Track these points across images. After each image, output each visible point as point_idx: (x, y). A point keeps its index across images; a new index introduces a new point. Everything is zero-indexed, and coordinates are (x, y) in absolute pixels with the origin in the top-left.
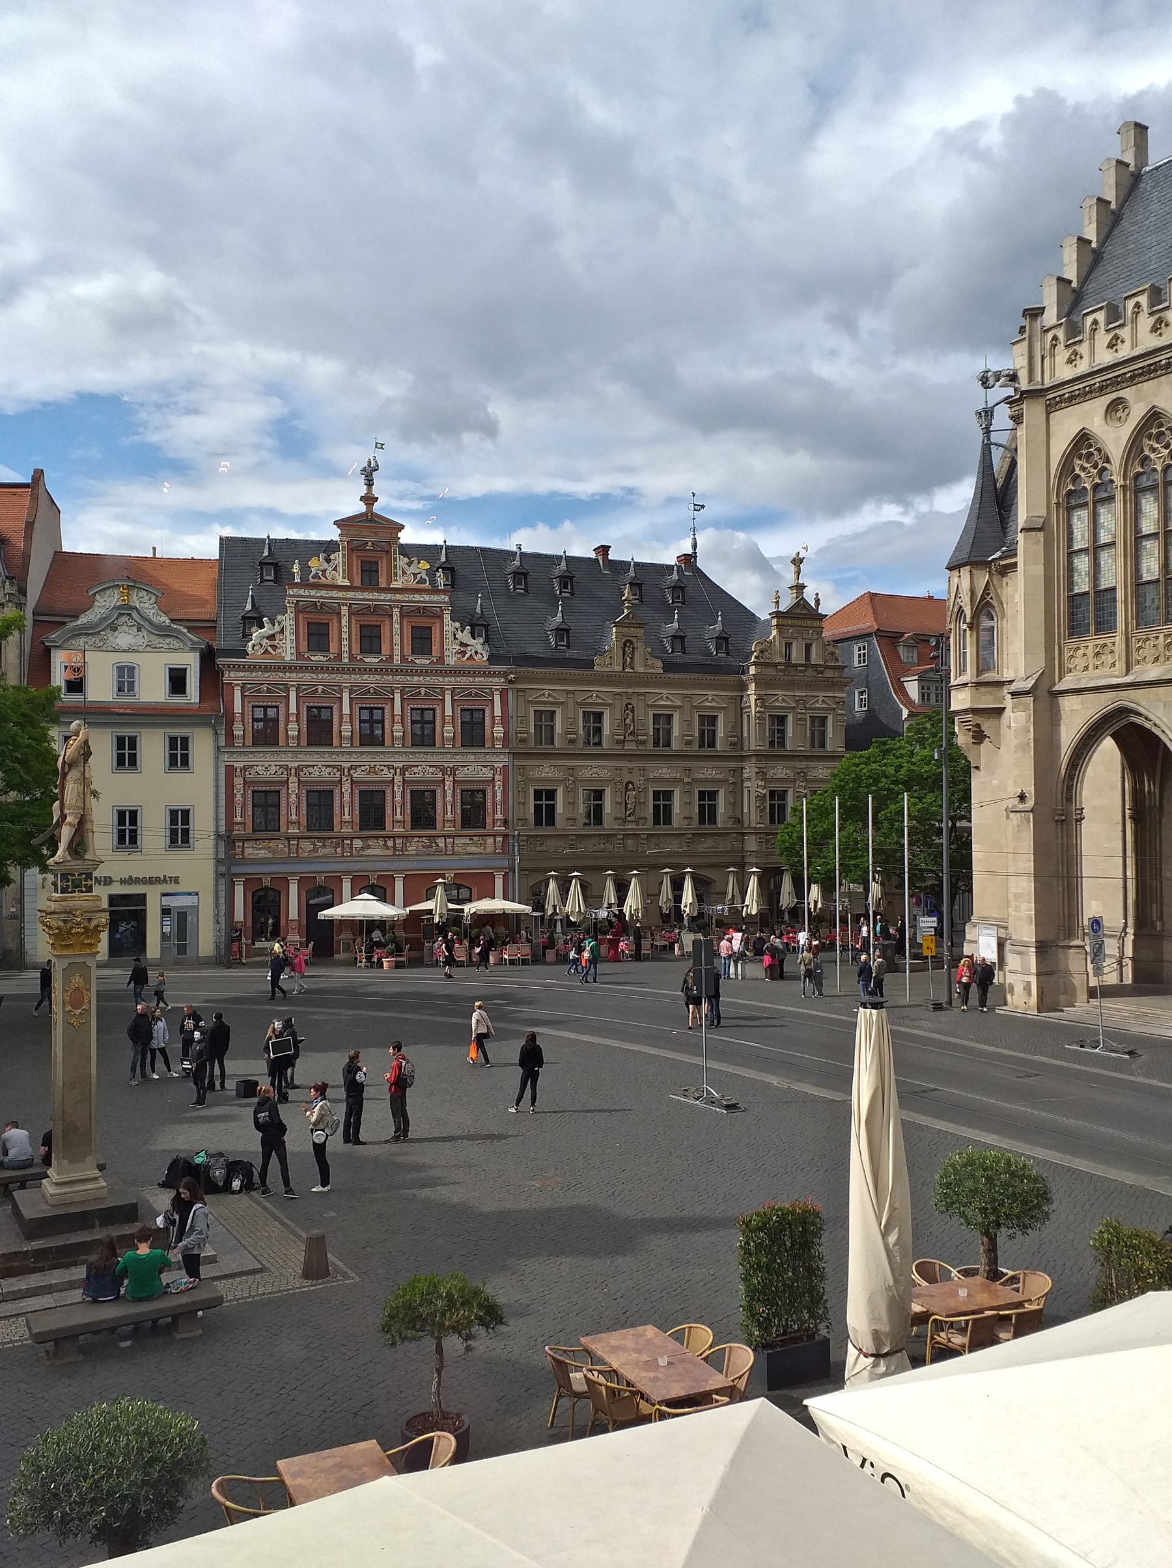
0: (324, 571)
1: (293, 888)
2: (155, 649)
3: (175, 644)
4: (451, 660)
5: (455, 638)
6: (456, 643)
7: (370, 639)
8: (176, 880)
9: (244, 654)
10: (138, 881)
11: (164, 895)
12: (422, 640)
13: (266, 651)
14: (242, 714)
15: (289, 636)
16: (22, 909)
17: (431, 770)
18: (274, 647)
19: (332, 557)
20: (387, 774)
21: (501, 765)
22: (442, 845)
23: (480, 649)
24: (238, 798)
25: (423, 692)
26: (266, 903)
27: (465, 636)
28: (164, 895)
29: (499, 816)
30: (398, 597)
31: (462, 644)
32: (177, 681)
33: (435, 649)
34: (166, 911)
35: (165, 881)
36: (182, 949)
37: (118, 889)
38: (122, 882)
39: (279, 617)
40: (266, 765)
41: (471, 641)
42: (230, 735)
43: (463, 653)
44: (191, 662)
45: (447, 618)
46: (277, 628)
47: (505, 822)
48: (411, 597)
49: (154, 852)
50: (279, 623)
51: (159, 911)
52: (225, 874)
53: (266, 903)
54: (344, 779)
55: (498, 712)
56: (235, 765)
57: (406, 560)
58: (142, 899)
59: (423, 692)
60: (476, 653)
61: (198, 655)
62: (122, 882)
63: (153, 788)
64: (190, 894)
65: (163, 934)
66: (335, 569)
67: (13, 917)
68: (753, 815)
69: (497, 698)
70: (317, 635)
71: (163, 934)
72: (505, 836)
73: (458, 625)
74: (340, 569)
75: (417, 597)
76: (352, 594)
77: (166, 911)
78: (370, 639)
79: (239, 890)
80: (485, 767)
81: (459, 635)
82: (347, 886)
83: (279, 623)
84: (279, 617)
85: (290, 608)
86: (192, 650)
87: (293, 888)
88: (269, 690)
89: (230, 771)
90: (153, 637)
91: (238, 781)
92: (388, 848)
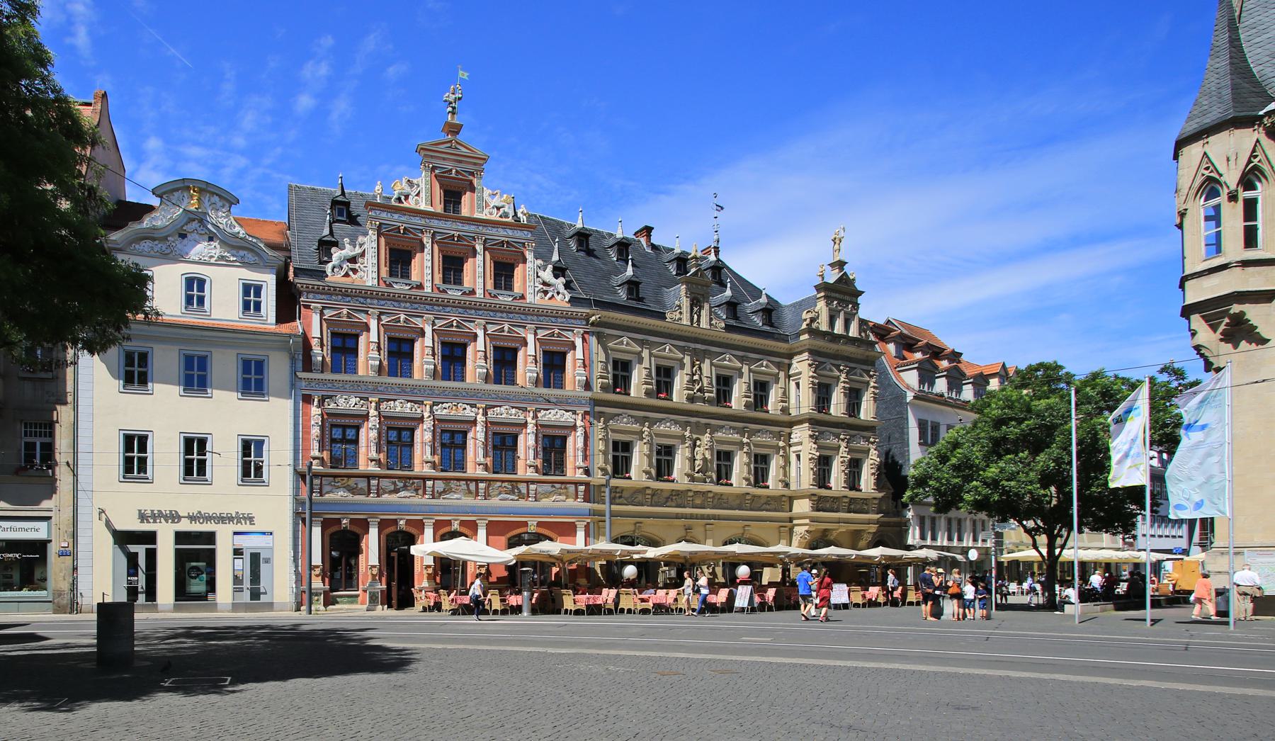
0: (407, 197)
1: (374, 532)
4: (533, 299)
6: (534, 281)
7: (452, 267)
9: (323, 274)
10: (209, 518)
11: (235, 533)
12: (503, 273)
13: (347, 275)
15: (370, 261)
17: (514, 411)
18: (355, 271)
20: (469, 413)
22: (524, 491)
25: (506, 329)
26: (343, 547)
27: (547, 275)
28: (235, 533)
29: (580, 463)
31: (544, 284)
34: (238, 552)
36: (255, 595)
37: (185, 526)
38: (192, 518)
39: (361, 239)
41: (553, 281)
43: (546, 293)
44: (269, 281)
46: (358, 250)
47: (587, 472)
49: (224, 485)
51: (231, 552)
52: (302, 517)
53: (343, 547)
58: (210, 537)
59: (506, 329)
62: (192, 518)
63: (225, 416)
64: (264, 533)
66: (418, 195)
69: (579, 342)
70: (399, 260)
73: (539, 262)
74: (423, 195)
76: (435, 223)
77: (238, 552)
78: (452, 267)
79: (317, 532)
82: (429, 532)
83: (361, 245)
84: (361, 239)
85: (372, 235)
87: (374, 532)
92: (470, 492)
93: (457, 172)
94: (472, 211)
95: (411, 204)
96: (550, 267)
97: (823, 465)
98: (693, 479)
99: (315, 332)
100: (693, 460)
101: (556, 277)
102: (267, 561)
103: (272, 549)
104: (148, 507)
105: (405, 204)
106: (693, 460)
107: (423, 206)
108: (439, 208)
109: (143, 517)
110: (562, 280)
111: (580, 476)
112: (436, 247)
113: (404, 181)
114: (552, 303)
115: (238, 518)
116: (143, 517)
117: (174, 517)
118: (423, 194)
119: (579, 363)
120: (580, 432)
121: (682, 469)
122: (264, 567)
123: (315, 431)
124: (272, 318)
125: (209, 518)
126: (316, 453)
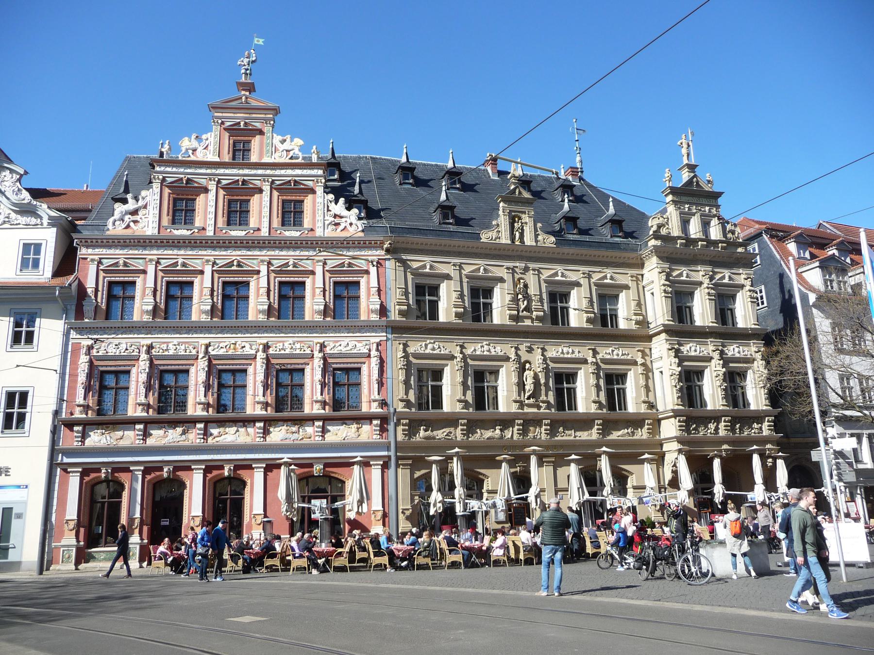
0: (194, 150)
2: (15, 226)
3: (33, 221)
5: (328, 210)
6: (326, 215)
7: (237, 212)
12: (291, 213)
13: (128, 227)
17: (298, 346)
18: (135, 222)
19: (204, 137)
20: (248, 351)
21: (378, 340)
23: (353, 219)
27: (340, 207)
30: (268, 172)
31: (335, 216)
32: (30, 254)
33: (307, 223)
39: (144, 193)
40: (114, 345)
41: (345, 213)
43: (338, 224)
44: (48, 238)
45: (320, 190)
46: (141, 203)
47: (383, 403)
48: (283, 172)
54: (201, 355)
55: (374, 283)
57: (280, 138)
59: (291, 263)
60: (351, 224)
61: (54, 230)
64: (19, 487)
68: (667, 396)
69: (373, 270)
72: (384, 420)
73: (331, 196)
74: (211, 148)
75: (289, 172)
78: (237, 212)
79: (74, 482)
80: (359, 341)
81: (332, 206)
83: (143, 198)
85: (156, 186)
88: (125, 264)
90: (13, 215)
92: (248, 434)
93: (246, 123)
94: (261, 156)
95: (200, 156)
96: (342, 200)
97: (689, 380)
98: (522, 405)
99: (90, 285)
100: (521, 385)
101: (349, 209)
102: (19, 516)
103: (25, 503)
105: (193, 158)
106: (521, 385)
107: (212, 157)
108: (227, 158)
110: (355, 211)
111: (375, 409)
112: (222, 193)
113: (193, 137)
114: (345, 234)
118: (209, 145)
119: (374, 291)
120: (374, 361)
121: (508, 397)
123: (82, 378)
124: (49, 273)
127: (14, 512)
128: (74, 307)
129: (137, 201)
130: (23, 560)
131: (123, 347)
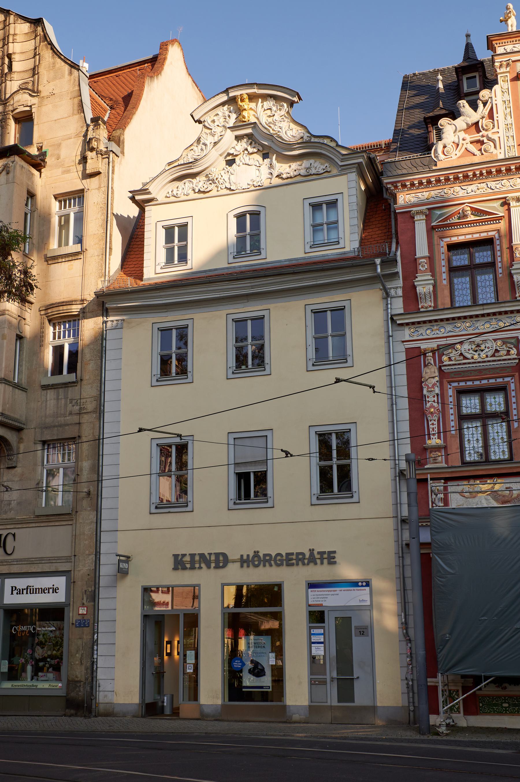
8: (330, 558)
10: (267, 560)
11: (312, 585)
14: (431, 259)
16: (95, 610)
24: (432, 402)
28: (312, 585)
34: (317, 617)
35: (312, 560)
37: (237, 574)
38: (244, 562)
39: (485, 94)
42: (411, 296)
50: (485, 104)
56: (424, 346)
62: (244, 562)
65: (313, 659)
67: (82, 623)
71: (313, 659)
77: (317, 617)
86: (344, 170)
89: (415, 358)
91: (430, 374)
104: (186, 549)
109: (179, 563)
115: (312, 558)
116: (179, 563)
117: (221, 561)
122: (357, 642)
125: (267, 560)
126: (434, 441)
127: (354, 624)
128: (400, 292)
129: (475, 107)
130: (379, 704)
131: (490, 345)
